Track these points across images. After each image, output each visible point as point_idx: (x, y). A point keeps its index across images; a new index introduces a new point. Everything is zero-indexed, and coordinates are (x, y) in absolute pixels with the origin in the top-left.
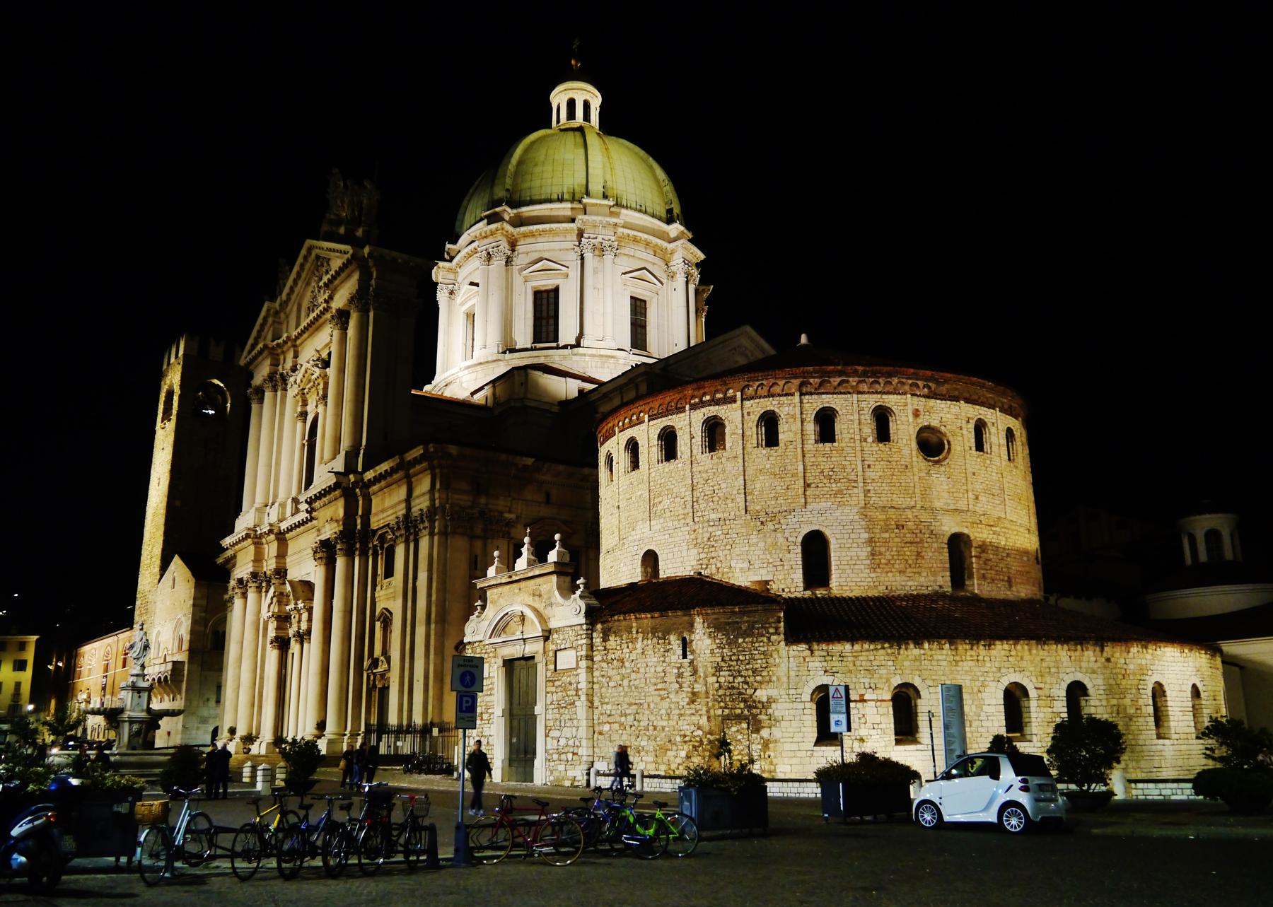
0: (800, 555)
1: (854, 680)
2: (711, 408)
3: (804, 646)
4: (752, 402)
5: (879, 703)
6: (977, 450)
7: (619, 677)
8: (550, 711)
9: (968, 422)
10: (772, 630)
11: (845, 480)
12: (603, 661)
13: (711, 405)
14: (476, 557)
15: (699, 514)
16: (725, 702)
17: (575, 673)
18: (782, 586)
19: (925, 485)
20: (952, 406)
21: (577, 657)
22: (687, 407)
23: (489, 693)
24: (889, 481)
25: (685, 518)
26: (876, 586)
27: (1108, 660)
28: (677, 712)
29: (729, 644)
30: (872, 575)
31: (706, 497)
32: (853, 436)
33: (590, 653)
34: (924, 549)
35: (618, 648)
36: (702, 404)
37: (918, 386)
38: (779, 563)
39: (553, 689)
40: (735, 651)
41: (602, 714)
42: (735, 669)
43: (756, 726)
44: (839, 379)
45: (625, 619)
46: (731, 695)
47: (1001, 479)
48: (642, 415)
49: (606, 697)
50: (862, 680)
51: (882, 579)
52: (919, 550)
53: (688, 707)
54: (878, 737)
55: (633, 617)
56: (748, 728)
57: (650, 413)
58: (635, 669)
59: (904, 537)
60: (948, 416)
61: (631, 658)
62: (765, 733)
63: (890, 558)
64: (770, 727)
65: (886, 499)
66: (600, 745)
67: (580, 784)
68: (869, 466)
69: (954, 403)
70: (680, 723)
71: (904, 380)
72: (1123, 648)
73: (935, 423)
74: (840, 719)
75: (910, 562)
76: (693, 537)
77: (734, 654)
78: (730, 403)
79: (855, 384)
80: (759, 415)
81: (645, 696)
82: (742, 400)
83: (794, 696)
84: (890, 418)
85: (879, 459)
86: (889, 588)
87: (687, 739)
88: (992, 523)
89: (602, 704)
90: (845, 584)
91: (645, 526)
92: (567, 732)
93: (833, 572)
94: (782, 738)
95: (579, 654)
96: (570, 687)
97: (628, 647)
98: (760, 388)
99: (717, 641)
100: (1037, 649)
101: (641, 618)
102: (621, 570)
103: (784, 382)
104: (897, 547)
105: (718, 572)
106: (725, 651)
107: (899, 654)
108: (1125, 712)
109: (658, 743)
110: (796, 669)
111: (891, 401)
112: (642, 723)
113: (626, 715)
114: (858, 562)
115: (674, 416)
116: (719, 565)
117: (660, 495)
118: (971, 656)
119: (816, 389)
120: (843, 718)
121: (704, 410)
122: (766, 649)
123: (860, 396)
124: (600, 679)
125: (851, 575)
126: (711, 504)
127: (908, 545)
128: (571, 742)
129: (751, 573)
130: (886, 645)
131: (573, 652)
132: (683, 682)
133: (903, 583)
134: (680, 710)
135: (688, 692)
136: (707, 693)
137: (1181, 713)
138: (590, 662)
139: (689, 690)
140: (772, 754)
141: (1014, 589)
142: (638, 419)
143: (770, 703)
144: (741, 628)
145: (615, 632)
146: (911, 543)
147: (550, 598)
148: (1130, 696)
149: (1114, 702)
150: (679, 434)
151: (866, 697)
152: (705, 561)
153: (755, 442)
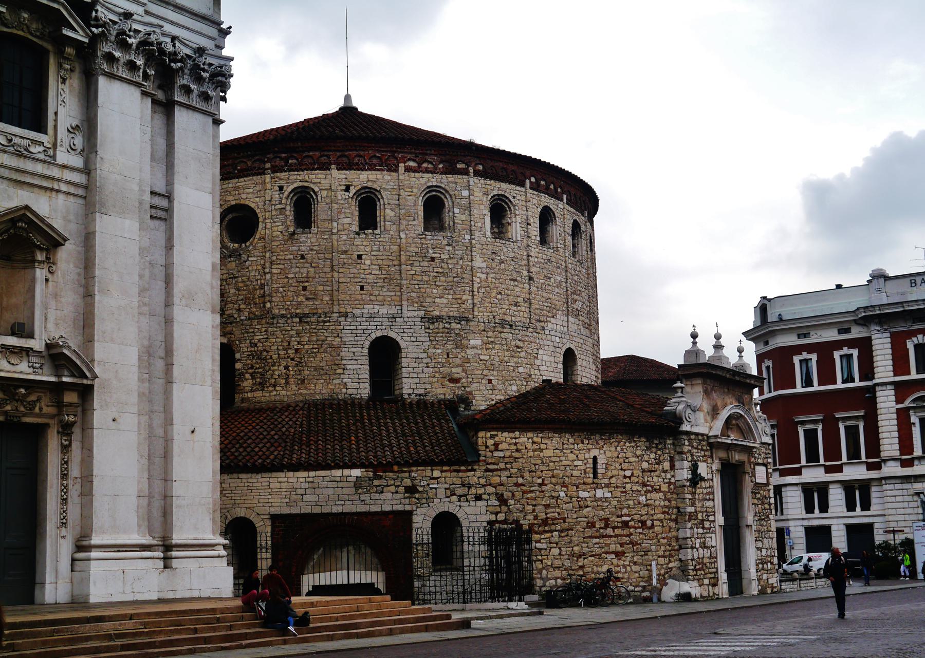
23: (708, 497)
39: (756, 501)
128: (769, 552)
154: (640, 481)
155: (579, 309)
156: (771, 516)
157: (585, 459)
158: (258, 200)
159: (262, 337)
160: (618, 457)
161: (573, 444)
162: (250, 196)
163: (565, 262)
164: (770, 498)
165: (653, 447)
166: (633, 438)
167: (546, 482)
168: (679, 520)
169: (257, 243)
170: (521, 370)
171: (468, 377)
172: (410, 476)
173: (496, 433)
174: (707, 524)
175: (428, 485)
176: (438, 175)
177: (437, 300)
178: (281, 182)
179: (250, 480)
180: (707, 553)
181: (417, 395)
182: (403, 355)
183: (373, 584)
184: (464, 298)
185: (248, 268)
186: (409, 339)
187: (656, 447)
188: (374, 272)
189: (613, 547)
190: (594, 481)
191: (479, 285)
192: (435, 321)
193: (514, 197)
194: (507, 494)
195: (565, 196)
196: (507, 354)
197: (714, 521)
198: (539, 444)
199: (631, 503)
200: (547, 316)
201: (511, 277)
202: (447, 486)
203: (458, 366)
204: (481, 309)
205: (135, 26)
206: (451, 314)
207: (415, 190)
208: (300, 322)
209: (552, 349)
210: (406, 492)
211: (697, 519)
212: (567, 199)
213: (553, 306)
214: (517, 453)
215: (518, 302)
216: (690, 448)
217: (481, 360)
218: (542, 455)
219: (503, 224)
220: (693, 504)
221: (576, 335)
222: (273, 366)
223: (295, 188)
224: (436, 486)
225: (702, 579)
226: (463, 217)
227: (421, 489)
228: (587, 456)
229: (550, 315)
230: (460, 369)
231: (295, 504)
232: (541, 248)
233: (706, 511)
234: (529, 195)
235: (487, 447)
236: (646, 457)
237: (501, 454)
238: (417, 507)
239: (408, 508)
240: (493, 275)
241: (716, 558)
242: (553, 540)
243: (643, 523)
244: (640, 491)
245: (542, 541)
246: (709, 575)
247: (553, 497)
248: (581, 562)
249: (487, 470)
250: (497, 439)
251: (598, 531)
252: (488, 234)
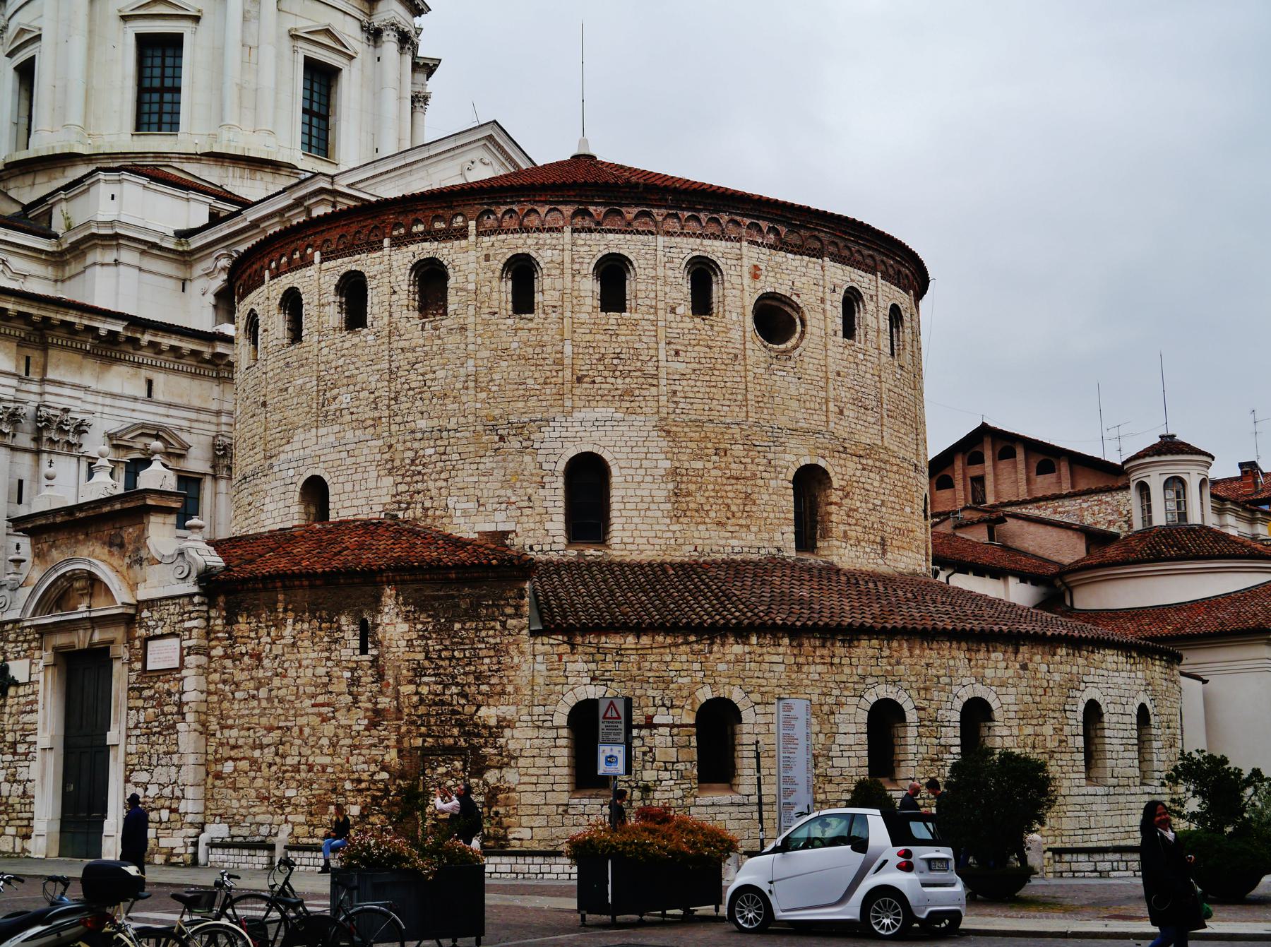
0: (561, 492)
1: (638, 692)
2: (427, 245)
3: (560, 637)
4: (493, 238)
5: (675, 731)
6: (844, 336)
7: (251, 684)
8: (133, 740)
9: (834, 291)
10: (509, 611)
11: (638, 373)
12: (226, 656)
13: (425, 241)
14: (21, 482)
15: (398, 419)
16: (428, 726)
17: (177, 676)
18: (529, 542)
19: (763, 388)
20: (811, 265)
21: (182, 649)
22: (386, 242)
23: (28, 708)
24: (707, 378)
25: (374, 426)
26: (680, 545)
27: (1024, 667)
28: (348, 741)
29: (438, 632)
30: (673, 528)
31: (411, 393)
32: (654, 303)
33: (204, 642)
34: (756, 490)
35: (253, 635)
36: (410, 238)
37: (760, 230)
38: (526, 504)
39: (140, 703)
40: (447, 643)
41: (222, 745)
42: (448, 672)
43: (479, 766)
44: (636, 210)
45: (265, 589)
46: (437, 714)
47: (879, 386)
48: (309, 251)
49: (229, 717)
50: (650, 693)
51: (689, 534)
52: (749, 491)
53: (367, 733)
54: (672, 782)
55: (279, 584)
56: (464, 770)
57: (324, 250)
58: (280, 670)
59: (727, 468)
60: (804, 279)
61: (274, 652)
62: (491, 776)
63: (703, 500)
64: (500, 768)
65: (701, 407)
66: (216, 796)
67: (180, 860)
68: (677, 353)
69: (814, 259)
70: (353, 760)
71: (738, 218)
72: (1047, 649)
73: (783, 290)
74: (615, 754)
75: (734, 508)
76: (386, 456)
77: (446, 649)
78: (458, 239)
79: (660, 219)
80: (504, 261)
81: (295, 716)
82: (479, 234)
83: (541, 718)
84: (714, 279)
85: (693, 342)
86: (699, 549)
87: (363, 785)
88: (861, 453)
89: (222, 728)
90: (631, 540)
91: (308, 435)
92: (161, 774)
93: (613, 520)
94: (520, 784)
95: (185, 644)
96: (168, 699)
97: (269, 634)
98: (507, 217)
99: (419, 626)
100: (923, 650)
101: (291, 588)
102: (265, 508)
103: (547, 207)
104: (716, 483)
105: (426, 516)
106: (430, 642)
107: (711, 652)
108: (1044, 747)
109: (314, 792)
110: (546, 673)
111: (715, 249)
112: (289, 761)
113: (262, 747)
114: (653, 506)
115: (364, 255)
116: (428, 504)
117: (335, 386)
118: (822, 657)
119: (598, 223)
120: (619, 751)
121: (413, 248)
122: (498, 640)
123: (666, 238)
124: (221, 686)
125: (640, 527)
126: (419, 403)
127: (733, 481)
128: (167, 792)
129: (481, 518)
130: (692, 638)
131: (175, 642)
132: (360, 694)
133: (722, 542)
134: (353, 738)
135: (367, 710)
136: (399, 710)
137: (1122, 748)
138: (203, 660)
139: (369, 705)
140: (502, 810)
141: (889, 555)
142: (302, 258)
143: (503, 728)
144: (459, 606)
145: (247, 610)
146: (737, 479)
147: (138, 550)
148: (1052, 721)
149: (1029, 730)
150: (371, 284)
151: (656, 720)
152: (406, 498)
153: (495, 303)
156: (180, 726)
174: (21, 748)
197: (35, 743)
225: (4, 827)
233: (23, 729)
246: (18, 822)
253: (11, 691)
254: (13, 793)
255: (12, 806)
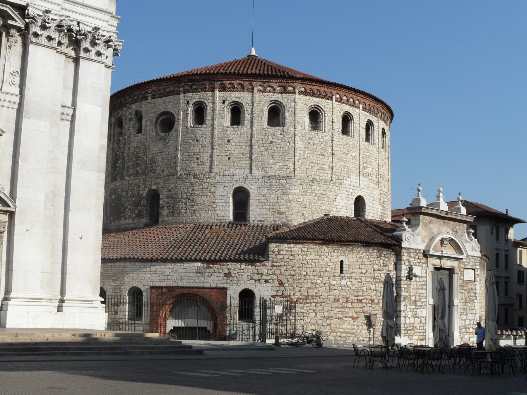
8: (461, 303)
23: (421, 287)
39: (463, 291)
92: (470, 316)
154: (372, 276)
155: (369, 172)
156: (475, 301)
157: (335, 262)
158: (175, 109)
159: (173, 186)
160: (357, 261)
161: (328, 253)
162: (172, 106)
163: (360, 144)
164: (476, 289)
165: (382, 256)
166: (369, 250)
167: (309, 274)
168: (398, 300)
169: (174, 133)
170: (324, 208)
171: (289, 211)
172: (227, 267)
173: (279, 244)
174: (419, 303)
175: (238, 273)
176: (277, 94)
177: (273, 166)
178: (188, 98)
179: (141, 266)
180: (417, 320)
181: (258, 221)
182: (251, 197)
183: (206, 328)
184: (289, 165)
185: (168, 147)
186: (255, 188)
187: (385, 256)
188: (237, 150)
189: (350, 314)
190: (341, 274)
191: (299, 158)
192: (271, 178)
193: (325, 106)
194: (284, 281)
195: (361, 106)
196: (315, 198)
198: (306, 252)
199: (365, 289)
200: (344, 176)
201: (320, 153)
202: (249, 274)
203: (283, 205)
204: (299, 172)
205: (52, 17)
206: (281, 174)
207: (262, 103)
208: (194, 178)
209: (347, 196)
210: (225, 276)
211: (411, 300)
212: (362, 107)
213: (349, 171)
214: (292, 257)
215: (324, 168)
216: (408, 257)
217: (298, 202)
218: (307, 258)
219: (318, 122)
220: (408, 291)
221: (365, 188)
222: (179, 202)
223: (196, 102)
224: (242, 274)
225: (412, 336)
226: (291, 118)
227: (233, 275)
228: (337, 260)
229: (346, 176)
230: (284, 207)
231: (163, 281)
232: (341, 136)
233: (419, 296)
234: (334, 105)
235: (273, 252)
236: (377, 262)
237: (282, 257)
238: (230, 285)
239: (225, 286)
240: (308, 152)
241: (426, 324)
242: (311, 308)
243: (372, 301)
244: (371, 282)
245: (305, 308)
246: (419, 334)
247: (313, 283)
248: (329, 321)
249: (273, 266)
250: (280, 248)
251: (341, 304)
252: (307, 128)
253: (414, 278)
254: (416, 322)
255: (416, 327)
